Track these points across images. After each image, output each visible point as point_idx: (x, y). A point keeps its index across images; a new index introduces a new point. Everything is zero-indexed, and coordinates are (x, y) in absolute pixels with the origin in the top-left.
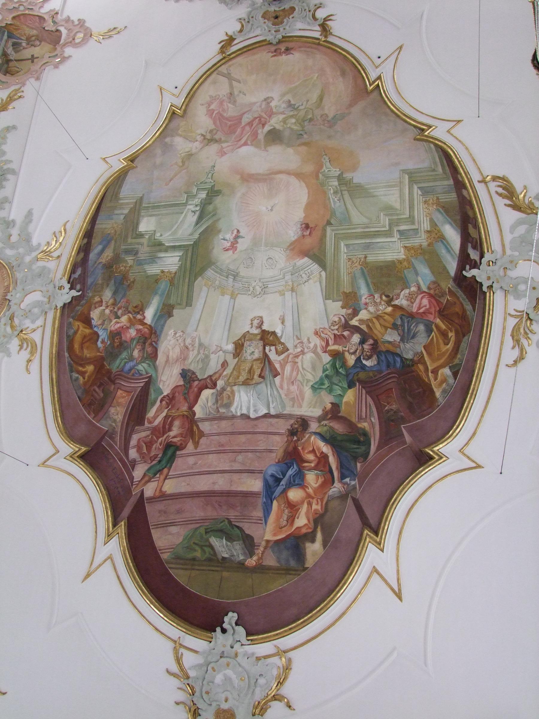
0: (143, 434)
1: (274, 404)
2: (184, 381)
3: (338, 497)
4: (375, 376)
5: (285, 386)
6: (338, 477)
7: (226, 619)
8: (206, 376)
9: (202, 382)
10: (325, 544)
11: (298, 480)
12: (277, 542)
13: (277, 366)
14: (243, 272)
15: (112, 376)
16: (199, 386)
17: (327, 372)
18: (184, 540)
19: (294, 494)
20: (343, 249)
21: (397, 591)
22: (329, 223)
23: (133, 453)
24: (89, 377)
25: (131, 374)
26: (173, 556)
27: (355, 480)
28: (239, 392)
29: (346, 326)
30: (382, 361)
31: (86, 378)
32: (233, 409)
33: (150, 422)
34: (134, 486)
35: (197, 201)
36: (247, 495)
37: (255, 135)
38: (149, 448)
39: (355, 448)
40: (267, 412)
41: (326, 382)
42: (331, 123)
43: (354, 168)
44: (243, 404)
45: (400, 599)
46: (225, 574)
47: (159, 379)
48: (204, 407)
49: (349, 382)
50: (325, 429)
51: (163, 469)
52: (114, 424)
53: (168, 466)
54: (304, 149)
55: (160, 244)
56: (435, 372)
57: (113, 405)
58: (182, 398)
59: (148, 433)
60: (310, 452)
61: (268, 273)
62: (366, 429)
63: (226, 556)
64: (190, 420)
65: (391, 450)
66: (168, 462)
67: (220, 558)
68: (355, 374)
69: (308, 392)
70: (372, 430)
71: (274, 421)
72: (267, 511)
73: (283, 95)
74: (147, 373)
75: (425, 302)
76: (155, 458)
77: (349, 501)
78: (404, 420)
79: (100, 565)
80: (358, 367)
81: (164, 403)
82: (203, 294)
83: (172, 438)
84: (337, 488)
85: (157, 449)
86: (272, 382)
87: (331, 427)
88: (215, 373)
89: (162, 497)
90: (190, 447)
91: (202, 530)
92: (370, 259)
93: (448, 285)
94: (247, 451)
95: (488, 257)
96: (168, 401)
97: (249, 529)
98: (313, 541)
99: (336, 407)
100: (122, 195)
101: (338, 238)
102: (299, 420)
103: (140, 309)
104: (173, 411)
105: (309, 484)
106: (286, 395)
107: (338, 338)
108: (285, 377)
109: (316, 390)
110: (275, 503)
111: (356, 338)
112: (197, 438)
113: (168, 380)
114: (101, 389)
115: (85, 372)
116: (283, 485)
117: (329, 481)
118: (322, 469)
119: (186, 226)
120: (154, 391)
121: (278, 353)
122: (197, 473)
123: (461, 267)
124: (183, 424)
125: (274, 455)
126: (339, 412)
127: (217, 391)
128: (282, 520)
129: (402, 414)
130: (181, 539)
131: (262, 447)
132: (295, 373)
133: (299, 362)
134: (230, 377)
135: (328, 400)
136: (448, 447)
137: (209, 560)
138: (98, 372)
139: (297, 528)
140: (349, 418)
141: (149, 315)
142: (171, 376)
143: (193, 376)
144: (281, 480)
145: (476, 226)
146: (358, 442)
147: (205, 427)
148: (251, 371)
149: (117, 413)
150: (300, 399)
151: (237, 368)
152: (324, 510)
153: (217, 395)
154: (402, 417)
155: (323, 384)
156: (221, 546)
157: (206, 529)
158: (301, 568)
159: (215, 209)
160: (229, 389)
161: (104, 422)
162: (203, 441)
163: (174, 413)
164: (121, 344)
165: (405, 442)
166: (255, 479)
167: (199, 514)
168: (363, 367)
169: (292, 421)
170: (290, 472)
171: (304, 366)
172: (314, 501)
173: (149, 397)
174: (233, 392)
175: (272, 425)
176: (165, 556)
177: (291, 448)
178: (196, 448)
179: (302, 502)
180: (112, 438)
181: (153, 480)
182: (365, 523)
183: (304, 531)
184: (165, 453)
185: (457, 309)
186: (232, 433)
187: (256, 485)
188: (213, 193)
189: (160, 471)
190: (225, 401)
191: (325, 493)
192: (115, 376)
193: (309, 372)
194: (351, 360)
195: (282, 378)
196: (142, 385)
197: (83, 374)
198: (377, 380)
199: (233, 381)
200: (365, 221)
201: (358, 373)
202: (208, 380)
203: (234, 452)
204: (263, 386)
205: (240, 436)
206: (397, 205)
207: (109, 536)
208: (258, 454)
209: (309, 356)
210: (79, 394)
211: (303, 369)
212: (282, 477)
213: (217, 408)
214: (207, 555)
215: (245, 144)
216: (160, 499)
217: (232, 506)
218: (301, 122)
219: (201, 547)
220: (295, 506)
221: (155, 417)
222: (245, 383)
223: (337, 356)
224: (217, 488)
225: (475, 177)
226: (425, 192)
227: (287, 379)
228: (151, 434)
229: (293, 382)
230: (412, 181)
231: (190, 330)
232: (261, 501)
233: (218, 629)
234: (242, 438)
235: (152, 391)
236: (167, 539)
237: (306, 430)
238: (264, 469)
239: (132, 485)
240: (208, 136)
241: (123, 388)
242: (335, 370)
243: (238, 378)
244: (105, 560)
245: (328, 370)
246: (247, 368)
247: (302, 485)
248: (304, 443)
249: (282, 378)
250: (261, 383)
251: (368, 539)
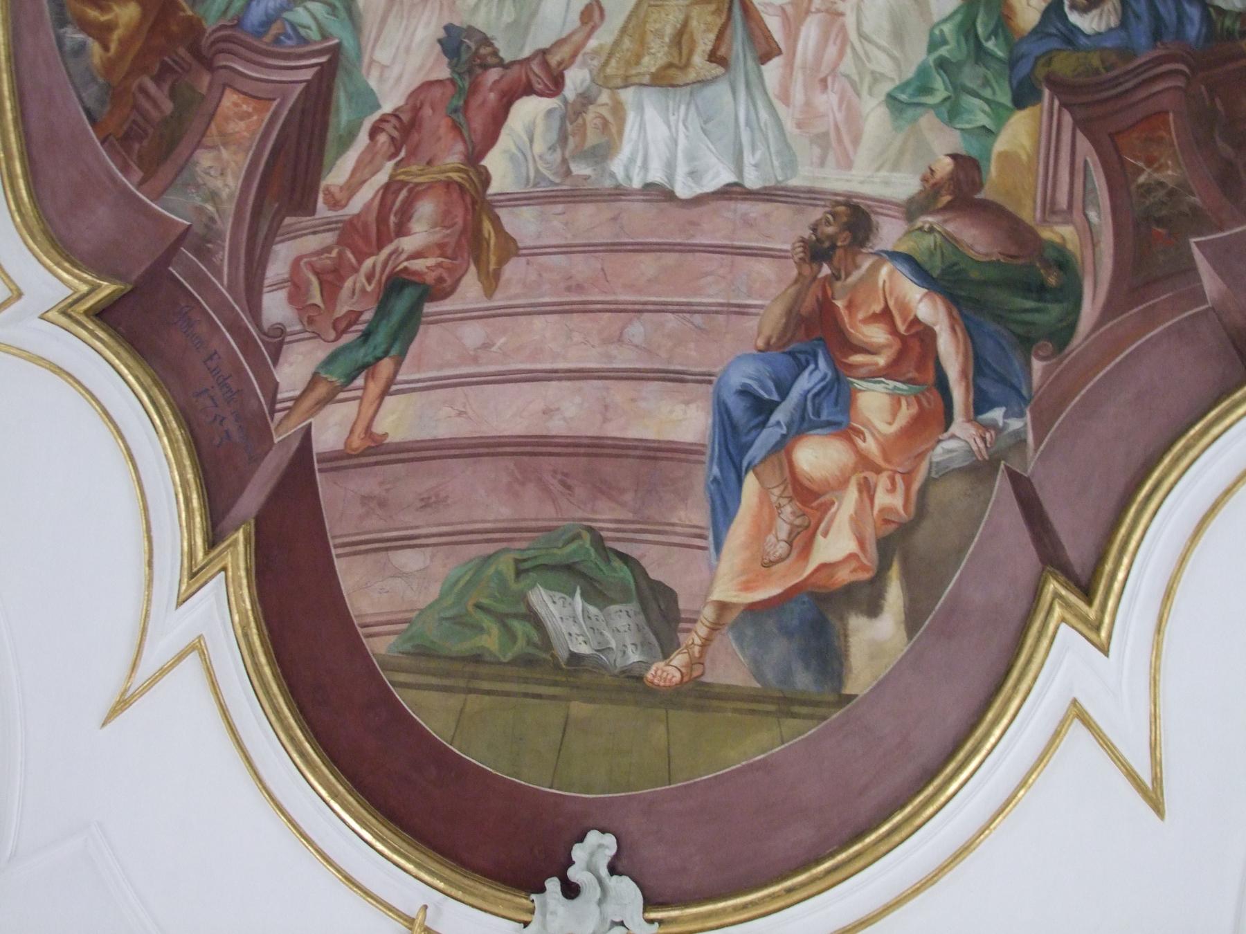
0: (311, 243)
1: (758, 154)
2: (453, 67)
3: (961, 471)
4: (1107, 70)
5: (798, 96)
6: (966, 407)
7: (579, 853)
8: (526, 53)
9: (515, 72)
10: (912, 621)
11: (832, 411)
12: (753, 609)
13: (774, 24)
15: (205, 42)
16: (504, 85)
17: (943, 51)
18: (442, 597)
19: (816, 456)
21: (1147, 778)
23: (276, 307)
24: (124, 44)
25: (268, 38)
26: (408, 647)
27: (1021, 415)
28: (640, 109)
30: (1138, 17)
31: (113, 46)
32: (617, 166)
33: (335, 204)
34: (278, 416)
38: (331, 286)
39: (1026, 311)
40: (731, 178)
41: (940, 84)
44: (652, 149)
45: (1157, 807)
46: (579, 709)
47: (366, 60)
48: (518, 159)
49: (1020, 83)
50: (929, 241)
51: (379, 359)
52: (210, 207)
53: (393, 352)
57: (207, 141)
58: (443, 125)
59: (329, 238)
60: (874, 318)
62: (1070, 246)
63: (584, 649)
64: (472, 199)
65: (1150, 319)
66: (394, 338)
67: (563, 655)
68: (1037, 58)
69: (874, 115)
70: (1088, 253)
71: (755, 209)
72: (724, 506)
74: (325, 37)
76: (350, 325)
77: (1001, 482)
78: (1198, 221)
79: (163, 671)
80: (1050, 35)
81: (382, 138)
83: (407, 259)
84: (961, 439)
85: (358, 293)
86: (753, 77)
87: (948, 238)
88: (560, 43)
89: (373, 451)
90: (470, 290)
91: (506, 565)
94: (662, 308)
96: (396, 134)
97: (661, 564)
98: (873, 609)
99: (967, 168)
102: (841, 209)
104: (414, 168)
105: (868, 424)
106: (799, 125)
108: (798, 61)
109: (901, 111)
110: (751, 483)
112: (493, 259)
113: (397, 63)
114: (166, 87)
115: (109, 27)
116: (778, 423)
118: (912, 374)
120: (350, 98)
122: (493, 377)
124: (446, 213)
125: (751, 323)
126: (978, 186)
127: (565, 101)
128: (771, 538)
129: (1196, 200)
130: (435, 591)
131: (712, 295)
132: (832, 51)
133: (848, 13)
134: (610, 55)
135: (941, 145)
137: (528, 661)
138: (153, 28)
139: (823, 566)
140: (1010, 208)
142: (408, 50)
143: (483, 51)
144: (771, 407)
146: (1039, 290)
147: (522, 224)
148: (681, 38)
149: (222, 171)
150: (847, 140)
152: (912, 509)
153: (563, 119)
154: (1194, 208)
155: (926, 90)
156: (567, 619)
157: (517, 561)
158: (831, 698)
160: (605, 97)
161: (172, 197)
162: (513, 270)
163: (417, 174)
165: (1200, 297)
166: (687, 403)
167: (499, 511)
168: (1071, 35)
169: (817, 214)
170: (806, 382)
171: (867, 28)
172: (883, 482)
173: (333, 120)
174: (618, 109)
175: (748, 223)
176: (379, 647)
177: (809, 304)
178: (489, 292)
179: (843, 483)
180: (203, 252)
181: (341, 395)
182: (1051, 557)
183: (844, 576)
184: (383, 309)
186: (614, 248)
187: (687, 421)
189: (367, 367)
190: (592, 138)
191: (921, 456)
192: (213, 43)
193: (884, 50)
195: (790, 65)
196: (308, 75)
197: (101, 32)
198: (1115, 82)
199: (621, 72)
201: (1048, 56)
202: (535, 67)
203: (617, 309)
204: (722, 88)
205: (642, 256)
207: (195, 575)
208: (698, 319)
210: (91, 104)
211: (862, 36)
212: (775, 397)
213: (564, 161)
214: (520, 646)
216: (364, 460)
217: (604, 489)
219: (502, 619)
220: (817, 495)
221: (352, 187)
222: (662, 80)
224: (556, 427)
227: (804, 68)
228: (340, 242)
229: (824, 81)
232: (703, 474)
233: (553, 885)
234: (648, 265)
235: (341, 97)
236: (386, 594)
237: (862, 245)
238: (717, 370)
239: (273, 412)
241: (240, 83)
242: (972, 41)
243: (638, 63)
244: (180, 657)
245: (944, 42)
246: (669, 31)
248: (855, 287)
249: (790, 65)
250: (715, 79)
251: (1058, 611)
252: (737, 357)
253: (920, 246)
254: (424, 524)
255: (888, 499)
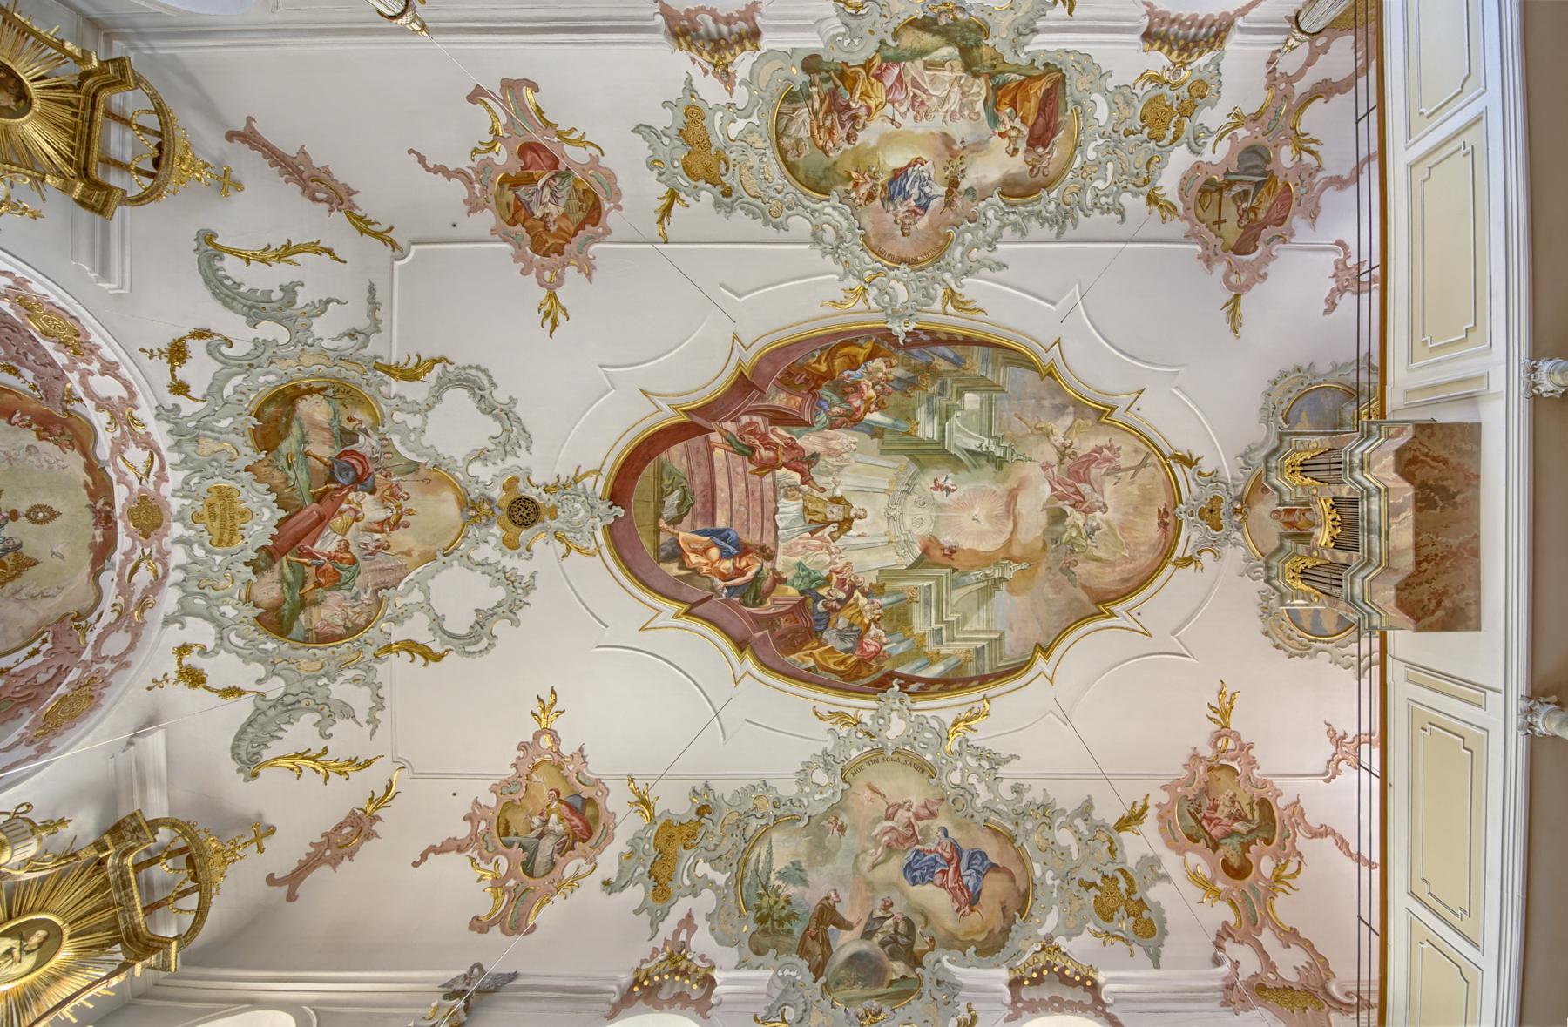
14: (911, 498)
19: (714, 553)
20: (927, 583)
22: (955, 570)
23: (745, 419)
29: (853, 587)
35: (992, 448)
36: (713, 516)
37: (1063, 498)
38: (750, 433)
42: (1066, 570)
43: (1011, 591)
48: (784, 476)
54: (1040, 545)
55: (947, 418)
56: (811, 655)
61: (908, 521)
64: (774, 465)
73: (1107, 523)
75: (872, 649)
78: (772, 632)
82: (891, 464)
84: (719, 584)
89: (710, 448)
90: (751, 467)
92: (915, 606)
93: (887, 666)
95: (908, 699)
97: (687, 520)
99: (784, 581)
100: (1009, 368)
101: (939, 579)
103: (880, 407)
107: (842, 582)
111: (842, 595)
117: (724, 577)
119: (966, 440)
121: (831, 534)
122: (730, 476)
123: (901, 677)
131: (751, 525)
135: (789, 575)
136: (750, 663)
141: (875, 417)
145: (941, 691)
147: (768, 479)
148: (816, 512)
151: (820, 501)
159: (981, 467)
162: (756, 478)
163: (781, 451)
164: (846, 394)
167: (697, 481)
168: (816, 601)
182: (694, 605)
185: (865, 672)
187: (721, 522)
188: (999, 463)
194: (823, 592)
197: (818, 362)
200: (954, 601)
206: (967, 628)
209: (828, 559)
215: (1053, 489)
217: (704, 505)
218: (1072, 542)
222: (805, 508)
223: (828, 580)
225: (990, 693)
226: (980, 652)
230: (990, 641)
231: (857, 455)
232: (709, 527)
240: (1069, 451)
247: (721, 558)
252: (738, 532)
253: (765, 571)
254: (693, 463)
255: (705, 570)
